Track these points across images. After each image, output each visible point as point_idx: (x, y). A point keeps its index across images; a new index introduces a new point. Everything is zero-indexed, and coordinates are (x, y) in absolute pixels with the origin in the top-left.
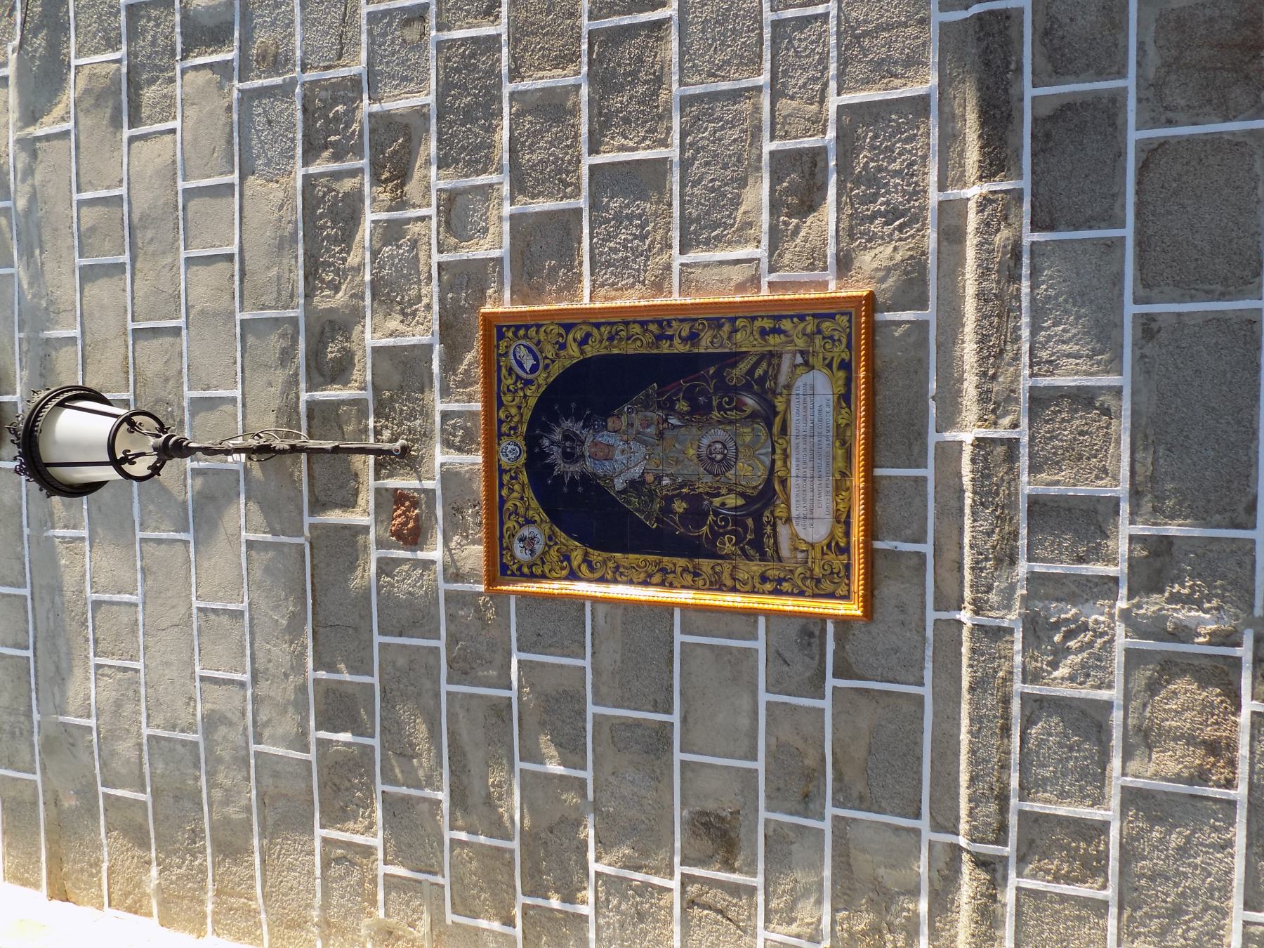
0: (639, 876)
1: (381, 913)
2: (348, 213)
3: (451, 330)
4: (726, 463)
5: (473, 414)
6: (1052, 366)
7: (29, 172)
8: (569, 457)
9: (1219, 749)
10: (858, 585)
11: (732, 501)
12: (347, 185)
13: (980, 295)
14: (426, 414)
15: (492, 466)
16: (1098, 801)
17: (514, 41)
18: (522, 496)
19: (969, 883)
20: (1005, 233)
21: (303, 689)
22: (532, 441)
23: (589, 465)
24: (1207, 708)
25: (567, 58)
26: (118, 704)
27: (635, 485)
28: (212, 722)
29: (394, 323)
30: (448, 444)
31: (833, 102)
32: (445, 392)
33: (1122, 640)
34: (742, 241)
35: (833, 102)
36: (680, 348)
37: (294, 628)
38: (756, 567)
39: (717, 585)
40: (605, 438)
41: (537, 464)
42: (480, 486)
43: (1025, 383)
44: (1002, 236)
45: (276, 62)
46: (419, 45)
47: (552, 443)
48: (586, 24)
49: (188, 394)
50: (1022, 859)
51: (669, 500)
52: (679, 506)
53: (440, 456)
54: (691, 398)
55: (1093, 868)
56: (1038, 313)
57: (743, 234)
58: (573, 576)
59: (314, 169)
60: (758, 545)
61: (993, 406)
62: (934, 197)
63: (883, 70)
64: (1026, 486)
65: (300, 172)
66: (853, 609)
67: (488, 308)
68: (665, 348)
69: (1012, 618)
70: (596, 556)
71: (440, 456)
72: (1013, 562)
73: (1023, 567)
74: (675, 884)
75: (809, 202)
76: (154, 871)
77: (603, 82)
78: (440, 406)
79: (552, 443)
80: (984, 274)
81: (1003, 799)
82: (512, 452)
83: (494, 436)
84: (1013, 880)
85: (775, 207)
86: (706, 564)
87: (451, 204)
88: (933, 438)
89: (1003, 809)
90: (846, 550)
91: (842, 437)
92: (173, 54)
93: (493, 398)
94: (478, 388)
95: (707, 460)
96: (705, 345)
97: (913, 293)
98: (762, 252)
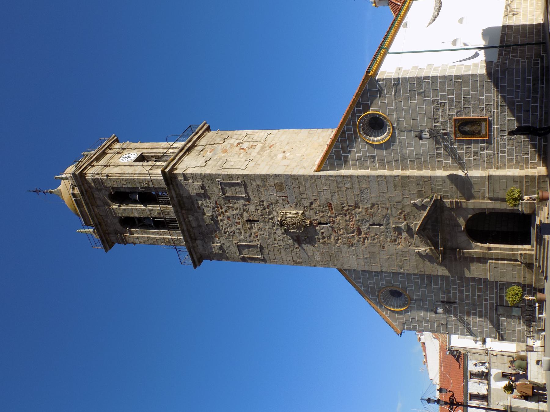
0: (469, 158)
1: (443, 165)
2: (438, 109)
3: (449, 119)
4: (476, 129)
5: (452, 126)
6: (502, 122)
7: (396, 105)
8: (462, 129)
9: (513, 145)
10: (488, 137)
11: (477, 131)
12: (438, 107)
13: (496, 118)
14: (447, 126)
15: (455, 130)
16: (506, 149)
17: (456, 97)
18: (458, 132)
19: (496, 155)
20: (498, 114)
21: (434, 148)
22: (458, 128)
23: (464, 129)
24: (512, 142)
25: (461, 99)
26: (411, 152)
27: (468, 131)
28: (423, 152)
29: (443, 119)
30: (450, 128)
31: (485, 104)
32: (449, 124)
33: (507, 139)
34: (478, 113)
35: (485, 104)
36: (472, 121)
37: (433, 143)
38: (479, 136)
39: (476, 137)
40: (465, 127)
41: (459, 130)
42: (454, 131)
43: (500, 123)
44: (498, 114)
45: (429, 97)
46: (446, 96)
47: (460, 128)
48: (463, 97)
49: (419, 125)
50: (500, 153)
51: (472, 131)
52: (472, 132)
53: (449, 129)
54: (473, 124)
55: (505, 153)
56: (501, 119)
57: (478, 113)
58: (463, 137)
59: (434, 106)
60: (479, 134)
61: (497, 125)
62: (493, 111)
63: (489, 102)
64: (500, 130)
65: (432, 106)
66: (487, 138)
67: (454, 118)
68: (471, 121)
69: (499, 138)
70: (465, 136)
71: (449, 129)
72: (499, 134)
73: (500, 135)
74: (472, 159)
75: (483, 110)
76: (416, 166)
77: (464, 101)
78: (449, 125)
79: (460, 128)
80: (497, 116)
81: (499, 149)
82: (457, 129)
83: (455, 127)
84: (500, 154)
85: (480, 111)
86: (475, 136)
87: (449, 110)
88: (493, 126)
89: (499, 150)
90: (486, 134)
91: (486, 127)
92: (416, 95)
93: (455, 124)
94: (453, 123)
95: (475, 129)
96: (474, 121)
97: (491, 117)
98: (479, 114)
